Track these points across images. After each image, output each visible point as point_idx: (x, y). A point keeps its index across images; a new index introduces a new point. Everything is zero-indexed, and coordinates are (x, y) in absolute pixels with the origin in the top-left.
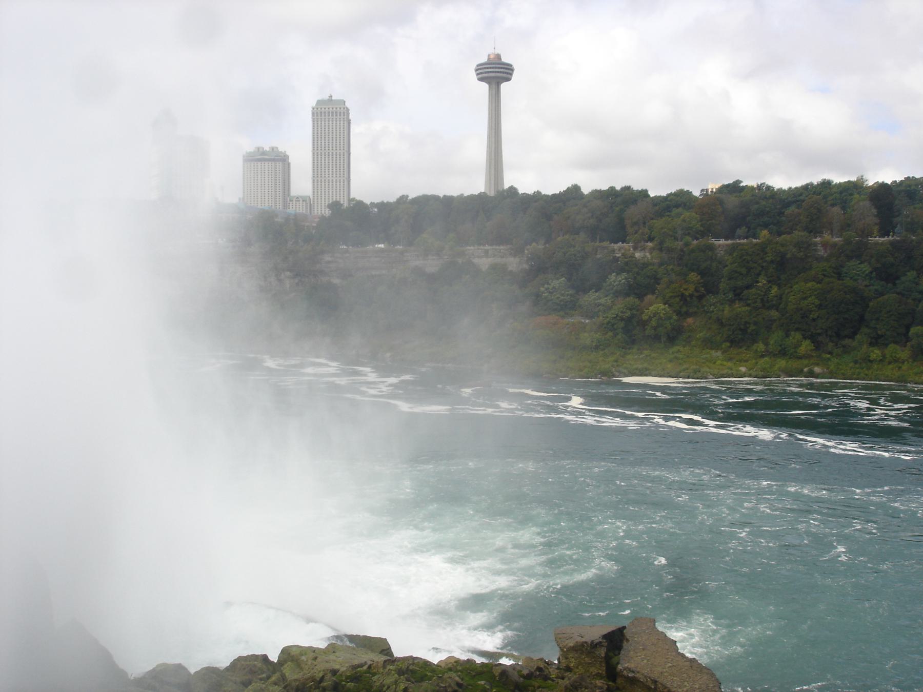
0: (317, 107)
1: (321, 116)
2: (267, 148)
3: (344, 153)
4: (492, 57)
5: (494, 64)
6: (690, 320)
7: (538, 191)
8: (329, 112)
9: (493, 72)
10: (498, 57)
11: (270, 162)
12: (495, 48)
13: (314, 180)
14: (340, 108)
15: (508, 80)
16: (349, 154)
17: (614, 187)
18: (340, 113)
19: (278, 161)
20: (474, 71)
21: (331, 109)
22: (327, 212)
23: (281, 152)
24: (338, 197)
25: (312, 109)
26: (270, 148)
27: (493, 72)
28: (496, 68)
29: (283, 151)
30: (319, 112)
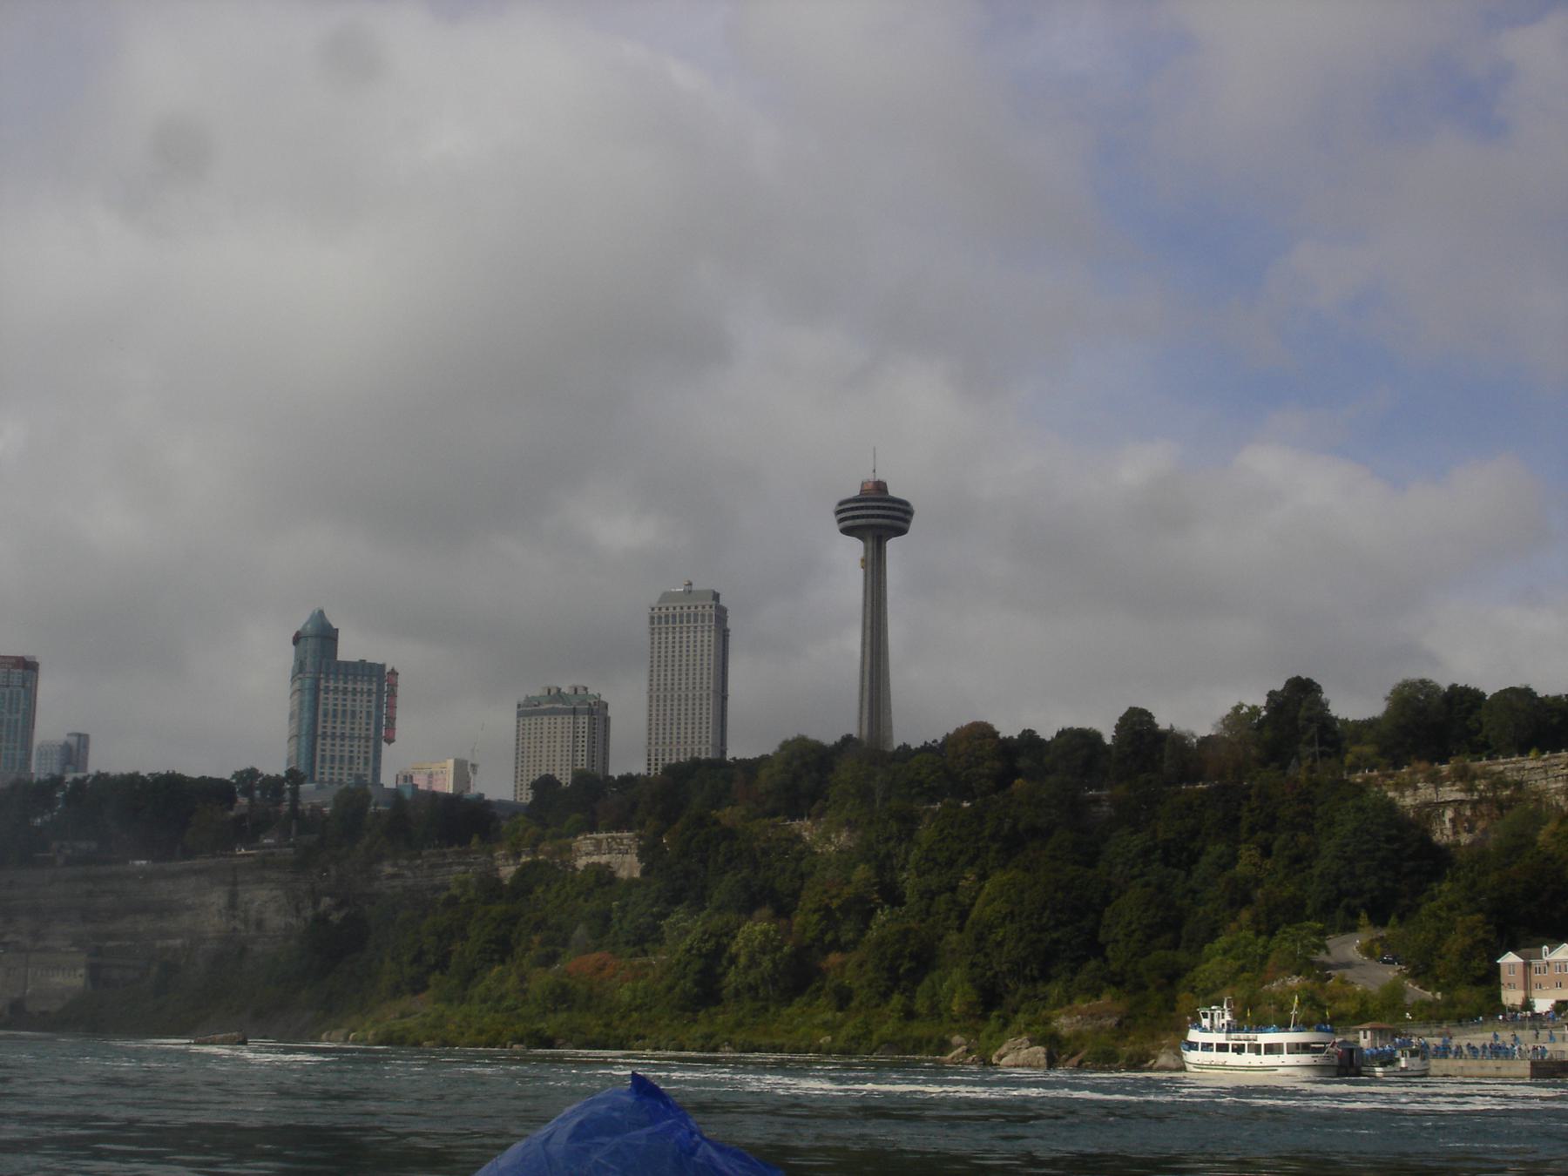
0: (660, 606)
1: (667, 622)
2: (565, 689)
3: (708, 695)
4: (866, 488)
5: (873, 500)
6: (834, 958)
7: (904, 744)
8: (681, 615)
9: (863, 517)
10: (880, 487)
11: (566, 717)
12: (874, 471)
13: (649, 750)
14: (704, 607)
15: (901, 531)
16: (724, 698)
17: (1034, 732)
18: (703, 615)
19: (597, 714)
20: (833, 515)
21: (671, 610)
22: (524, 796)
24: (551, 768)
26: (571, 687)
27: (863, 517)
28: (867, 508)
29: (596, 694)
30: (663, 616)
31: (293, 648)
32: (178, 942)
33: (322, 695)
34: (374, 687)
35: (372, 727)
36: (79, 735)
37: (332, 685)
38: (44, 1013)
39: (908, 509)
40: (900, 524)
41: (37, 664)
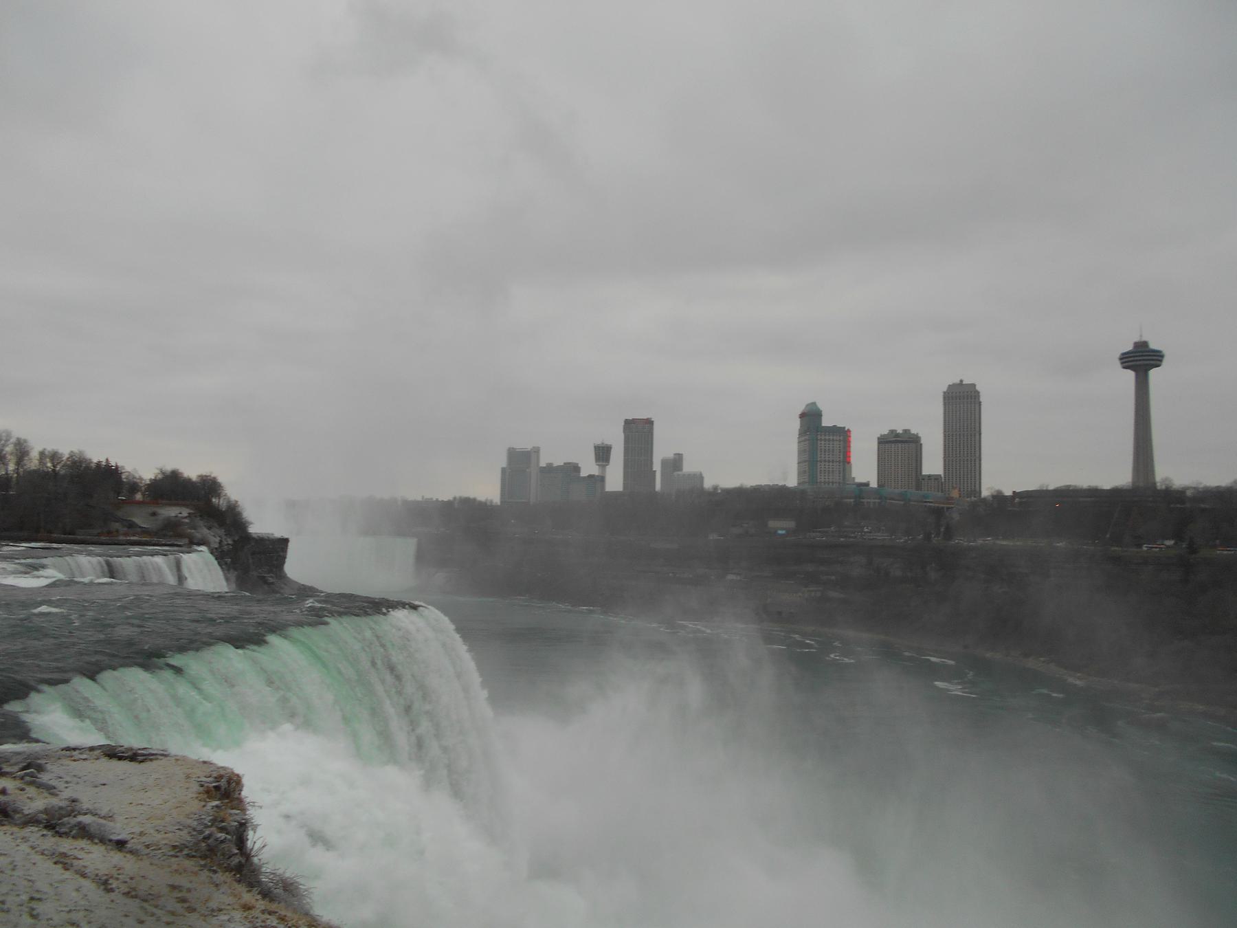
2: (900, 431)
10: (1145, 344)
15: (1158, 366)
18: (971, 396)
23: (914, 434)
25: (942, 394)
31: (799, 419)
32: (833, 578)
33: (819, 442)
34: (841, 438)
35: (841, 456)
36: (679, 454)
37: (823, 437)
38: (780, 613)
39: (1161, 354)
40: (1158, 362)
41: (653, 421)
